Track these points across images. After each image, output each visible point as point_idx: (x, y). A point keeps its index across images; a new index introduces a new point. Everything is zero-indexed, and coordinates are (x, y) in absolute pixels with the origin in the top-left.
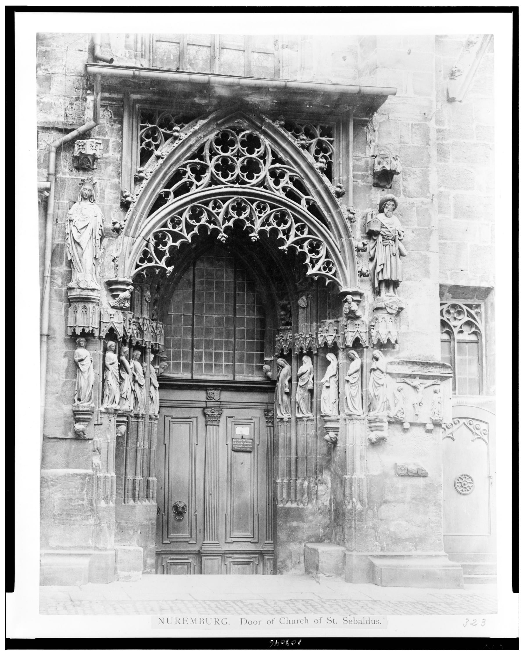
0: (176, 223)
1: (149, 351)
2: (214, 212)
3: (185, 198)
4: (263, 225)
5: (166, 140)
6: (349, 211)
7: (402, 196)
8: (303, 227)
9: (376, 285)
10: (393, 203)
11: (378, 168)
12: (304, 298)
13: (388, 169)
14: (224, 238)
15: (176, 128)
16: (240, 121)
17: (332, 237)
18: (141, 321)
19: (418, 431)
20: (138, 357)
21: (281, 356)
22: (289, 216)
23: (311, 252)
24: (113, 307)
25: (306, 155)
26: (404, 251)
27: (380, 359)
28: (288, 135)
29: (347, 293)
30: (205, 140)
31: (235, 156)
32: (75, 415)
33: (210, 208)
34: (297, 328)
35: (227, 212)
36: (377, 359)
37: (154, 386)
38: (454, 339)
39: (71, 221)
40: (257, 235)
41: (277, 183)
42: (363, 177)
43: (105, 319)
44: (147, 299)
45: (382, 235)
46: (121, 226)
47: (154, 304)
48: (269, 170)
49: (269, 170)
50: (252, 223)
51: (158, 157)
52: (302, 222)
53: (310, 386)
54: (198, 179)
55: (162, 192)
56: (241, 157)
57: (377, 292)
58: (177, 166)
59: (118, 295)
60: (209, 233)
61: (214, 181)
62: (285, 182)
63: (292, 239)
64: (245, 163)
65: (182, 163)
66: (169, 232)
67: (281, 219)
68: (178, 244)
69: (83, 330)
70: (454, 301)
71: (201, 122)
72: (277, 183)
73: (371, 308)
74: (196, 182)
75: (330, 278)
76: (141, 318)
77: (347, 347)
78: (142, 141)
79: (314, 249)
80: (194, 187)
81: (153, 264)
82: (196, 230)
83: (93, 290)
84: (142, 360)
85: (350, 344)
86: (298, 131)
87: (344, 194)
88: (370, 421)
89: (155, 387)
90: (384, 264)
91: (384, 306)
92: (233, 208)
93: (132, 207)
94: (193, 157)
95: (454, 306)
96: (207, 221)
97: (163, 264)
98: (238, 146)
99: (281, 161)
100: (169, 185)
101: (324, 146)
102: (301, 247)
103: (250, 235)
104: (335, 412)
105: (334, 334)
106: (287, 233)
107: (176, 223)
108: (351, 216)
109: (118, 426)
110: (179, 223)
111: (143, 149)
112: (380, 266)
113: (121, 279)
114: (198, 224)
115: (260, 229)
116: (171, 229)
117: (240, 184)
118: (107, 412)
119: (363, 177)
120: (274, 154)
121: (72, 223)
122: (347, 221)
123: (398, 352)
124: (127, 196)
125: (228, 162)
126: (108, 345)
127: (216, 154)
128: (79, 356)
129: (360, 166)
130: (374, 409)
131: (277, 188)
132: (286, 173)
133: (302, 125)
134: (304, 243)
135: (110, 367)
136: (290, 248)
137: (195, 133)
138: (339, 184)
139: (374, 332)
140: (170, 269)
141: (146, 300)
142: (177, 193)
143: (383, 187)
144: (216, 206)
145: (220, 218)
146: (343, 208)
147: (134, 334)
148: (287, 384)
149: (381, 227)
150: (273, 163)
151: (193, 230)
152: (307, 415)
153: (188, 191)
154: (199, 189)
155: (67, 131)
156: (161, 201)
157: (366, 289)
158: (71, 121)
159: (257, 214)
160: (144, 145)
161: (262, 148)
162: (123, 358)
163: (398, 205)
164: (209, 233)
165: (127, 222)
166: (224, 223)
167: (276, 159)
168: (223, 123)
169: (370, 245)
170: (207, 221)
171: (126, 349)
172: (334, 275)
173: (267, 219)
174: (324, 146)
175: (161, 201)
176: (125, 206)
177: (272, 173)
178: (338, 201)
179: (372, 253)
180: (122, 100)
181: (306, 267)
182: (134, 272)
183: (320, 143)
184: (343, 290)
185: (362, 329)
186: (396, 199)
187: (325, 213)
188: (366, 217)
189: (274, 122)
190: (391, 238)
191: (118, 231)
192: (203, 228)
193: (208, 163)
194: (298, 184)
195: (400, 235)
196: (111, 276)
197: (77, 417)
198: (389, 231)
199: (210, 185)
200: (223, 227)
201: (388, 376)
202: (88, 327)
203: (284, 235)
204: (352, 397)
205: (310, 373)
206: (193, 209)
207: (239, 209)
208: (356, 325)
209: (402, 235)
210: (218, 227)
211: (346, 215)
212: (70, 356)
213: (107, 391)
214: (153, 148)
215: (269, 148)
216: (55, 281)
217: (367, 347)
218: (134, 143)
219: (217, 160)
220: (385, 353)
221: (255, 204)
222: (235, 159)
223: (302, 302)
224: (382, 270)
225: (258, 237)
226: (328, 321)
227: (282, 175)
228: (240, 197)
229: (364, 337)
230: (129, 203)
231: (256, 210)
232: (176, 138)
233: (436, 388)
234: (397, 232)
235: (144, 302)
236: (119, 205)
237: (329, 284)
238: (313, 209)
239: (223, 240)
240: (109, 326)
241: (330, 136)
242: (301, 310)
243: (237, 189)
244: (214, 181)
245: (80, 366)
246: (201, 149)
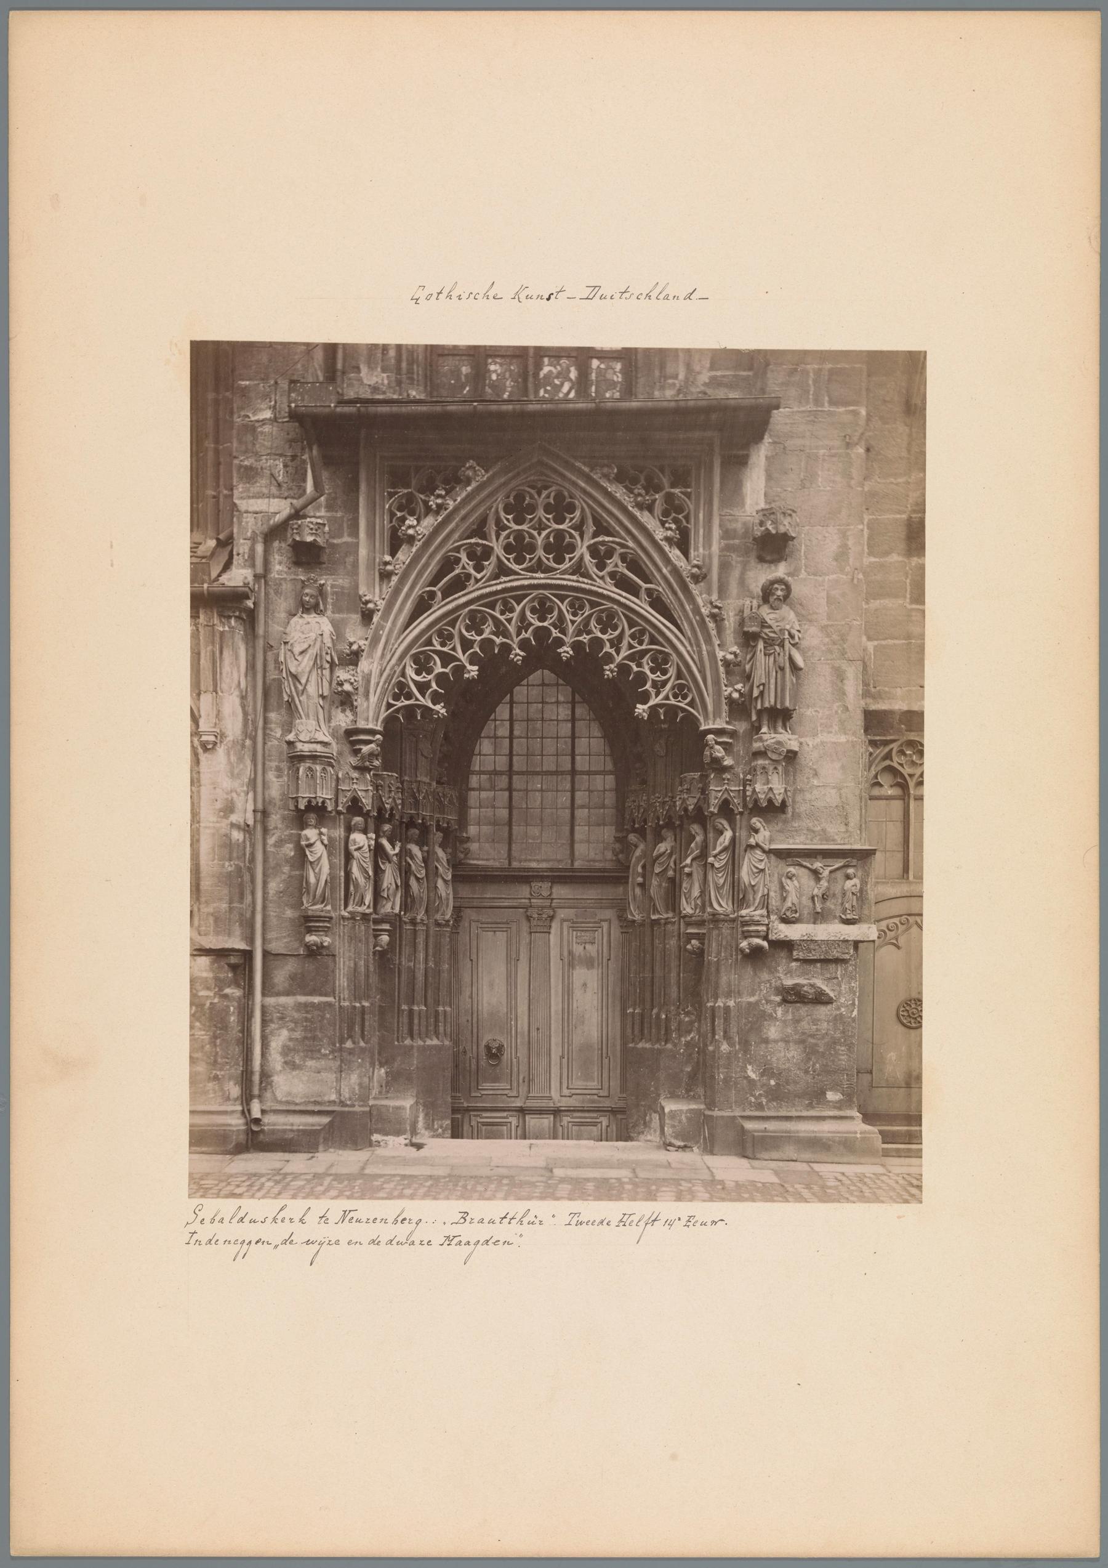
2: (502, 618)
4: (579, 633)
10: (783, 587)
14: (518, 657)
18: (414, 786)
22: (620, 619)
24: (355, 768)
26: (799, 660)
28: (619, 492)
29: (710, 731)
31: (535, 530)
35: (523, 617)
37: (443, 878)
39: (286, 643)
40: (569, 649)
44: (425, 754)
45: (763, 638)
46: (360, 647)
48: (589, 547)
49: (589, 547)
50: (563, 632)
52: (640, 625)
53: (671, 873)
54: (479, 568)
55: (423, 593)
56: (544, 529)
59: (361, 749)
60: (496, 651)
61: (502, 570)
62: (614, 563)
63: (624, 653)
64: (551, 539)
65: (449, 546)
67: (608, 623)
69: (309, 802)
72: (601, 566)
75: (683, 710)
76: (416, 781)
78: (392, 515)
80: (472, 581)
84: (422, 842)
85: (714, 809)
86: (635, 481)
89: (445, 881)
90: (764, 685)
91: (763, 749)
92: (533, 611)
93: (376, 619)
101: (677, 502)
102: (639, 665)
103: (560, 650)
105: (698, 796)
106: (616, 643)
107: (445, 638)
108: (716, 611)
110: (451, 637)
112: (758, 687)
114: (479, 638)
116: (439, 648)
117: (542, 572)
120: (597, 521)
121: (289, 647)
125: (524, 539)
126: (353, 823)
127: (505, 528)
128: (308, 839)
129: (735, 530)
131: (601, 574)
132: (615, 549)
133: (641, 472)
134: (642, 658)
135: (356, 854)
138: (695, 562)
141: (422, 755)
142: (447, 592)
145: (512, 629)
147: (396, 805)
149: (763, 627)
150: (595, 535)
151: (472, 648)
154: (480, 584)
159: (569, 617)
162: (385, 842)
163: (792, 587)
164: (496, 651)
167: (602, 529)
171: (387, 827)
172: (692, 704)
174: (677, 502)
177: (593, 550)
182: (383, 715)
183: (669, 497)
184: (703, 728)
188: (743, 612)
189: (592, 470)
190: (778, 643)
193: (494, 544)
194: (634, 566)
195: (792, 636)
198: (774, 632)
200: (516, 640)
202: (315, 798)
203: (611, 648)
205: (670, 855)
208: (724, 779)
209: (796, 638)
210: (511, 642)
216: (273, 733)
217: (741, 813)
219: (508, 537)
220: (767, 821)
222: (535, 533)
224: (762, 693)
225: (571, 652)
227: (610, 553)
228: (541, 591)
231: (568, 611)
234: (787, 633)
237: (682, 718)
239: (518, 660)
243: (540, 578)
245: (308, 853)
246: (483, 521)
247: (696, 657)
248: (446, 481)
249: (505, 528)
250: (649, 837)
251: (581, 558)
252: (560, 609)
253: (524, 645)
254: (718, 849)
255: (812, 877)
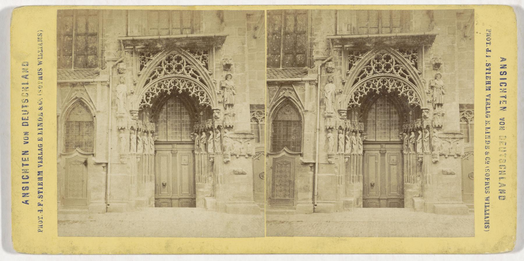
0: (361, 88)
1: (150, 133)
2: (374, 84)
3: (156, 80)
4: (392, 87)
5: (358, 60)
6: (423, 79)
7: (235, 73)
8: (407, 86)
9: (225, 106)
11: (224, 64)
12: (202, 112)
13: (228, 63)
15: (360, 55)
16: (174, 51)
17: (416, 88)
19: (242, 158)
20: (354, 135)
21: (196, 132)
23: (201, 96)
24: (341, 119)
25: (197, 61)
27: (436, 133)
30: (371, 58)
32: (328, 156)
33: (373, 82)
34: (200, 122)
36: (435, 133)
38: (259, 124)
41: (397, 71)
42: (220, 67)
43: (338, 123)
47: (360, 117)
51: (145, 67)
54: (369, 72)
57: (225, 109)
58: (361, 69)
61: (374, 73)
66: (359, 92)
67: (399, 84)
68: (362, 96)
70: (468, 110)
71: (369, 52)
73: (433, 114)
74: (159, 74)
77: (215, 129)
78: (349, 61)
79: (202, 95)
80: (367, 75)
81: (145, 104)
82: (368, 90)
83: (332, 113)
87: (212, 74)
88: (224, 155)
94: (367, 65)
95: (468, 111)
96: (372, 87)
97: (357, 103)
98: (383, 60)
99: (189, 65)
100: (359, 76)
104: (421, 151)
105: (420, 124)
107: (361, 88)
109: (345, 159)
110: (362, 88)
111: (349, 64)
113: (342, 109)
114: (369, 88)
115: (391, 88)
118: (339, 154)
119: (429, 67)
122: (213, 84)
123: (443, 130)
124: (343, 80)
130: (434, 151)
135: (340, 139)
136: (402, 94)
137: (158, 58)
139: (224, 123)
140: (360, 104)
142: (361, 78)
143: (227, 70)
144: (376, 81)
145: (377, 86)
146: (211, 79)
148: (406, 142)
152: (413, 153)
153: (365, 77)
154: (369, 76)
155: (116, 61)
156: (356, 81)
157: (430, 107)
158: (325, 57)
159: (390, 83)
160: (141, 63)
161: (182, 61)
165: (135, 90)
166: (378, 87)
168: (377, 52)
169: (222, 91)
170: (372, 87)
173: (394, 85)
175: (356, 81)
176: (344, 84)
178: (210, 77)
179: (223, 94)
180: (341, 48)
181: (199, 101)
185: (220, 122)
186: (441, 74)
187: (415, 81)
191: (341, 92)
192: (371, 89)
194: (405, 71)
195: (442, 87)
196: (131, 109)
197: (225, 156)
199: (373, 74)
200: (378, 89)
201: (230, 139)
204: (426, 147)
206: (367, 83)
207: (384, 82)
211: (213, 82)
212: (326, 135)
213: (339, 148)
214: (144, 64)
215: (184, 60)
218: (346, 62)
221: (389, 80)
223: (201, 114)
226: (209, 120)
227: (399, 69)
229: (430, 125)
230: (136, 83)
232: (360, 59)
233: (458, 142)
235: (355, 116)
236: (341, 84)
238: (411, 80)
240: (339, 125)
241: (207, 54)
242: (410, 116)
244: (374, 73)
246: (370, 62)
247: (420, 92)
248: (361, 53)
249: (375, 63)
250: (408, 134)
251: (393, 70)
252: (388, 81)
253: (379, 90)
254: (426, 137)
255: (449, 143)
